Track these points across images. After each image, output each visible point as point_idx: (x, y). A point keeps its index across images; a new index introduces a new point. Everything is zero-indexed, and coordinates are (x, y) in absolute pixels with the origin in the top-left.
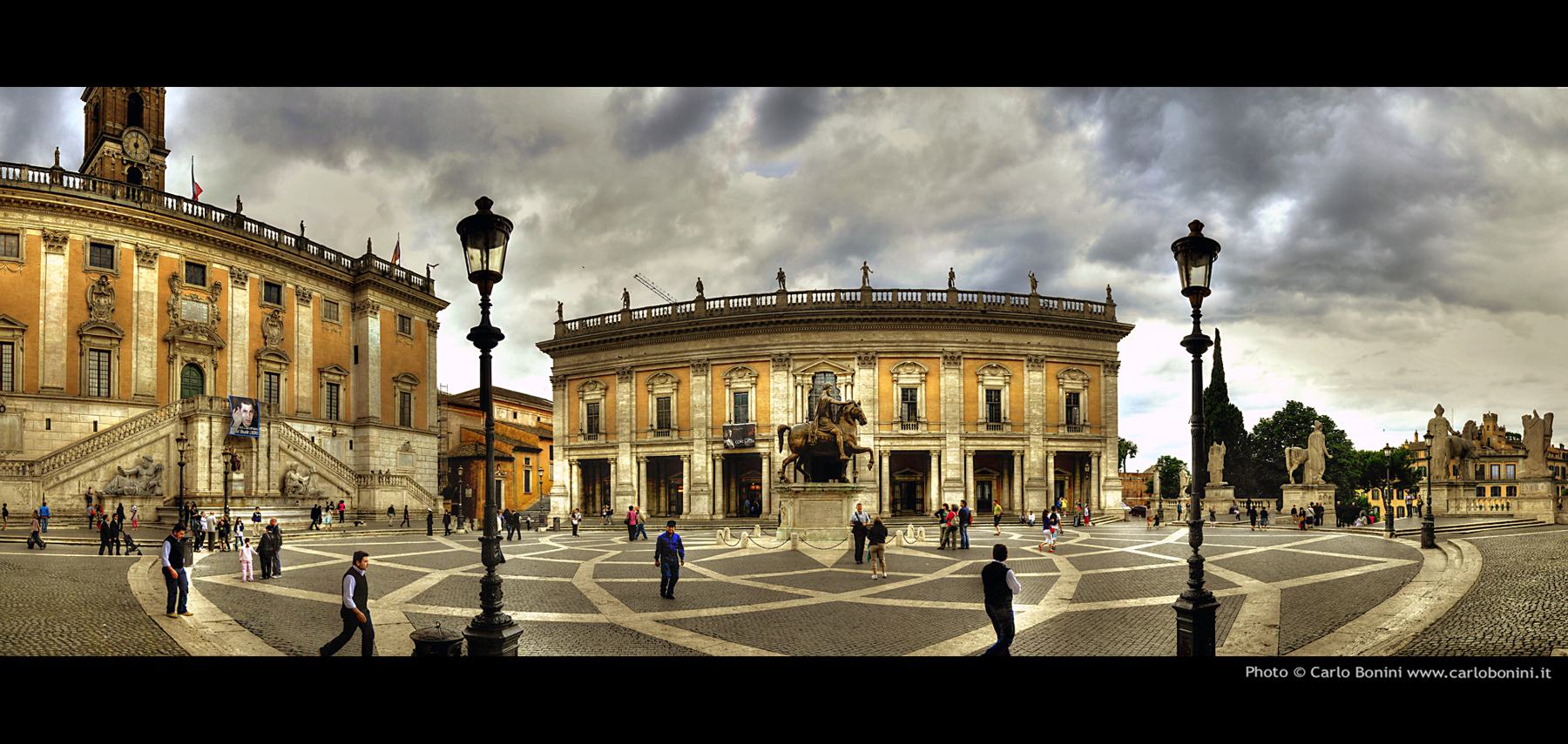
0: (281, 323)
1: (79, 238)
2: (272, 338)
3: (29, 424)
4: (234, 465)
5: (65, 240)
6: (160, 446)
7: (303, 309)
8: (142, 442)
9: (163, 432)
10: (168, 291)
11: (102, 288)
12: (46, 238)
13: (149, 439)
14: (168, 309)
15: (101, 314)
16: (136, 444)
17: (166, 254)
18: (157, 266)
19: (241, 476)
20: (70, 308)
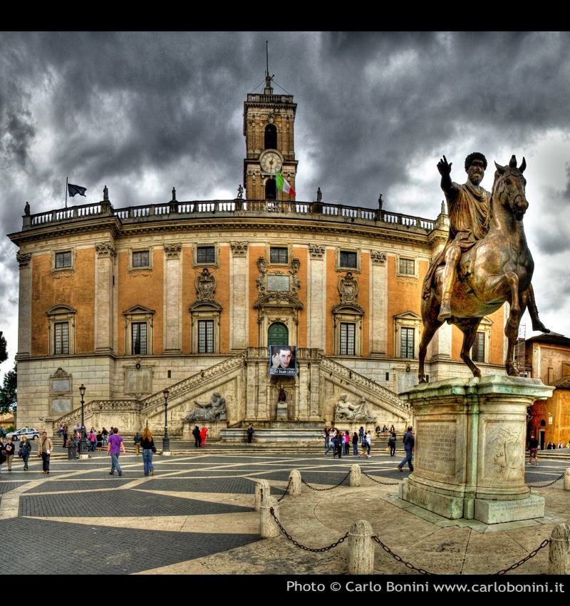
0: (355, 283)
1: (189, 245)
2: (347, 296)
3: (156, 375)
4: (282, 398)
5: (179, 249)
6: (231, 385)
7: (377, 269)
8: (216, 383)
9: (231, 376)
10: (257, 271)
11: (205, 278)
12: (166, 250)
13: (220, 381)
14: (257, 284)
15: (205, 296)
16: (211, 385)
17: (254, 245)
18: (247, 255)
19: (285, 405)
20: (184, 294)
